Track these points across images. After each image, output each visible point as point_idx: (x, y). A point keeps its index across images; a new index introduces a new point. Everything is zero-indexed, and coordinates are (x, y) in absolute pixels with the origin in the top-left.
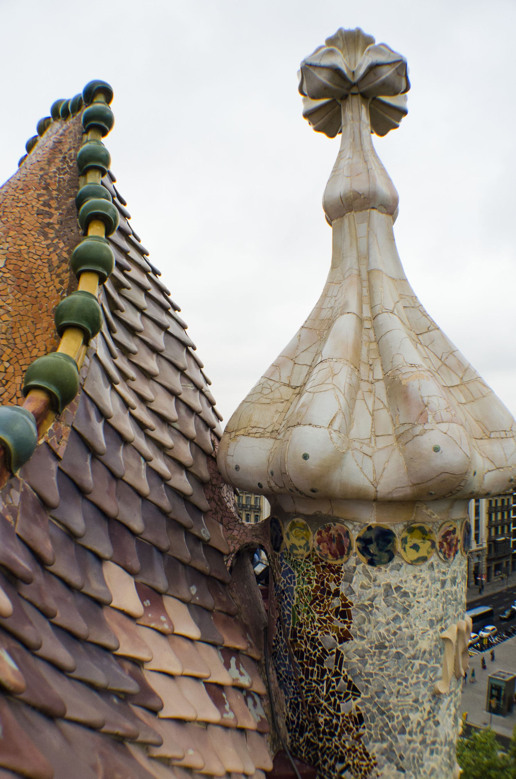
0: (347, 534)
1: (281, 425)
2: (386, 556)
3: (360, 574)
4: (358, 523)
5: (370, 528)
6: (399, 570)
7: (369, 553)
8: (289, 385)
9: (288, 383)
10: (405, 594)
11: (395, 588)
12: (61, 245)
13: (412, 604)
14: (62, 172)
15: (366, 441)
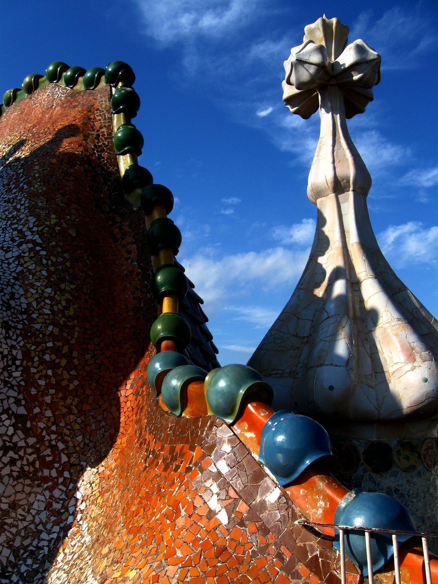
1: (297, 367)
3: (367, 480)
5: (372, 443)
6: (396, 476)
8: (296, 336)
9: (295, 334)
10: (402, 495)
11: (395, 491)
12: (118, 219)
13: (408, 503)
14: (99, 150)
15: (369, 377)
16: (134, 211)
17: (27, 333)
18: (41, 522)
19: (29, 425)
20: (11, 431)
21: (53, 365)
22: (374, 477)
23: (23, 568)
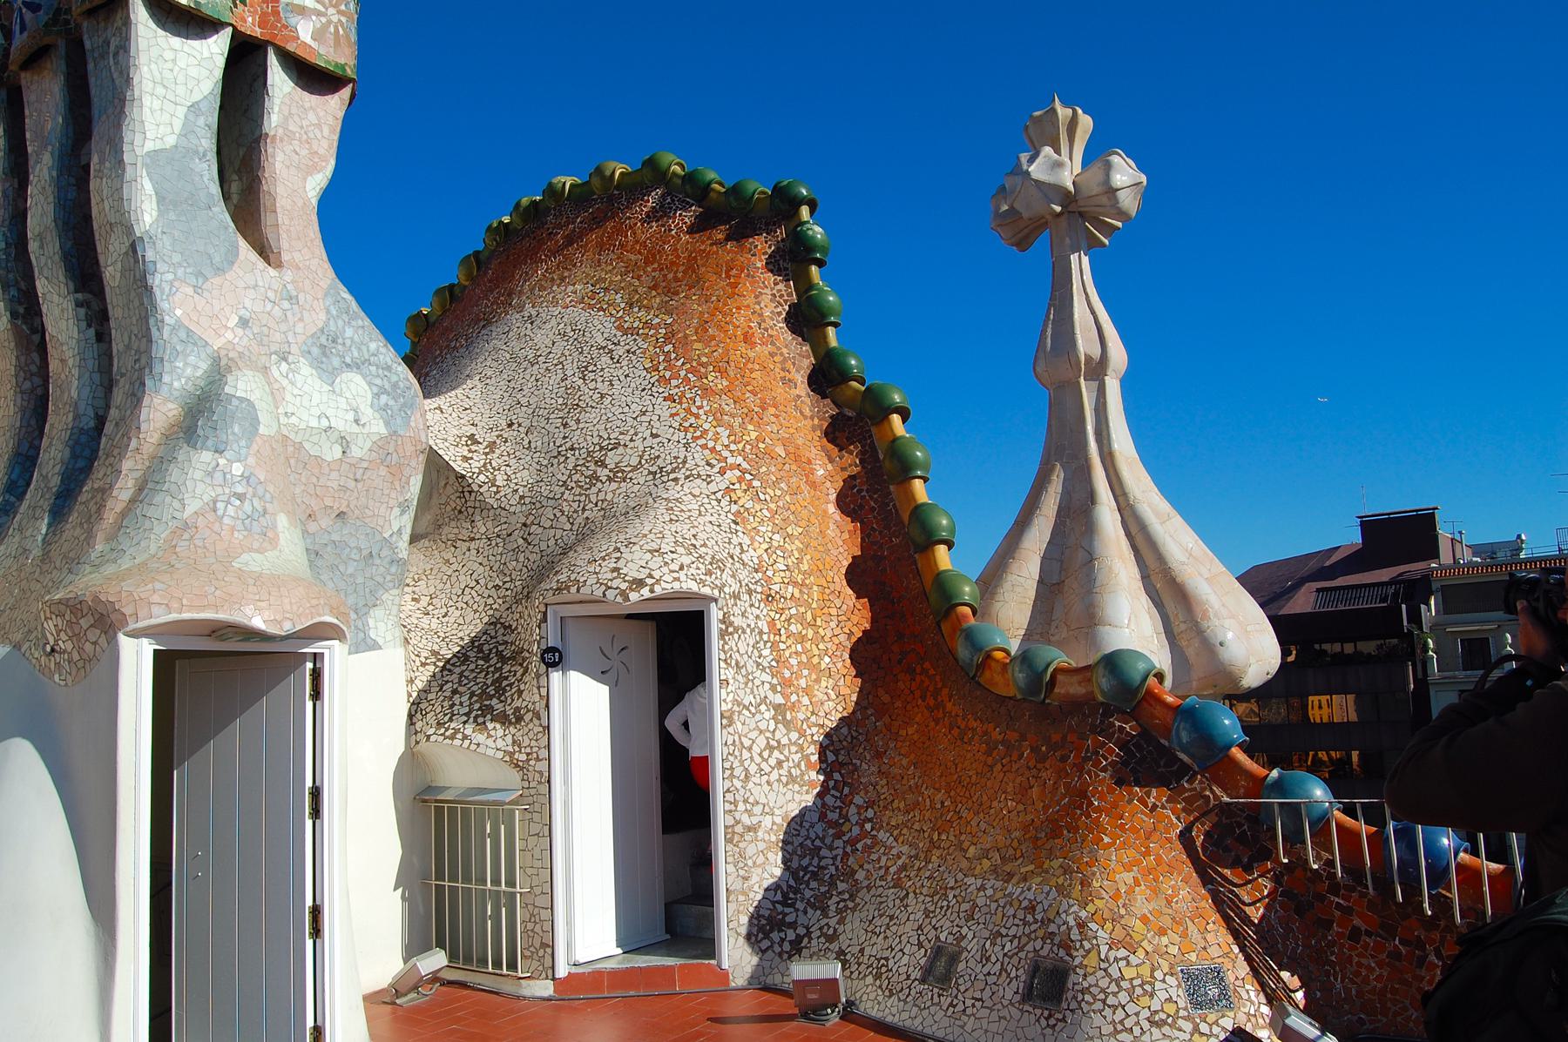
16: (850, 418)
17: (769, 598)
18: (817, 837)
19: (789, 717)
20: (772, 722)
21: (802, 639)
23: (808, 893)
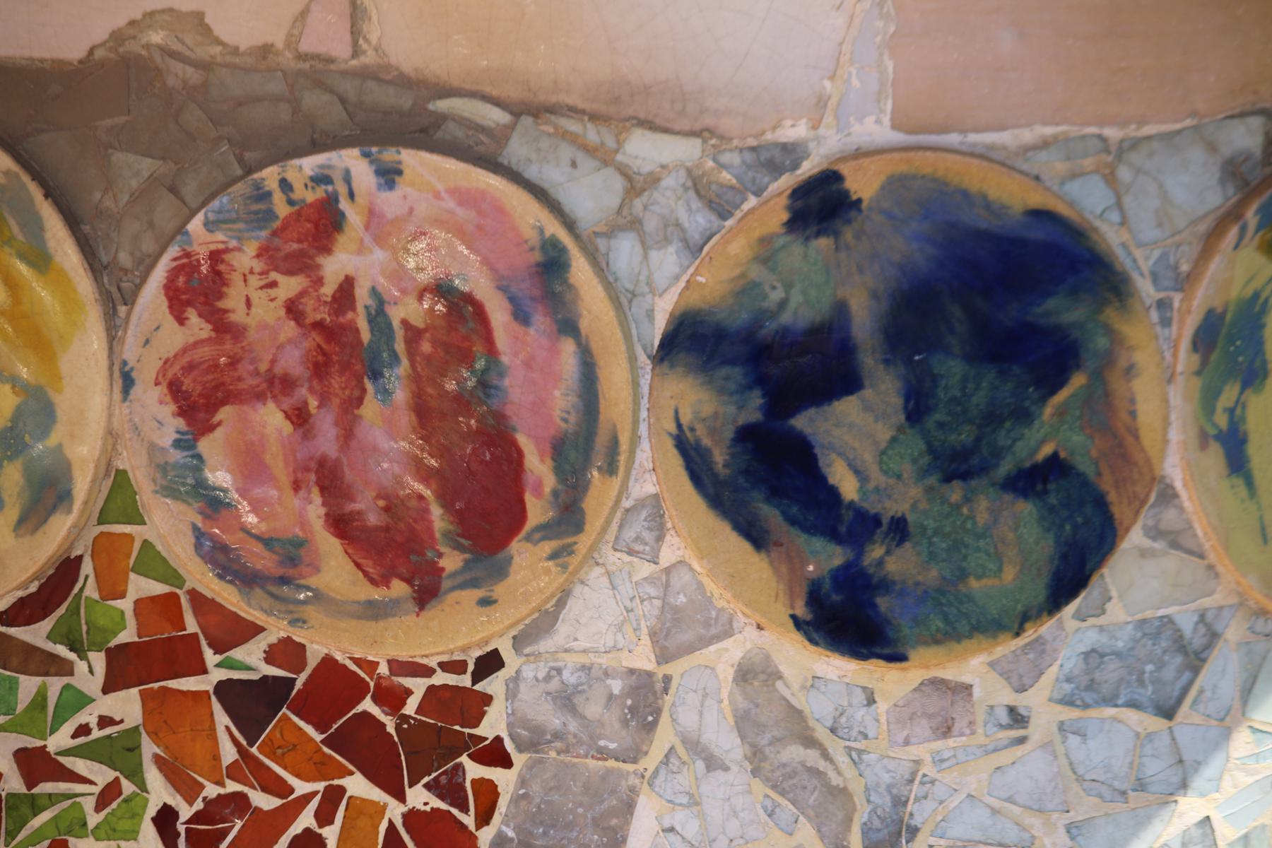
0: (546, 280)
2: (1019, 535)
3: (713, 763)
4: (683, 151)
5: (821, 204)
6: (1168, 712)
7: (817, 506)
22: (819, 709)
